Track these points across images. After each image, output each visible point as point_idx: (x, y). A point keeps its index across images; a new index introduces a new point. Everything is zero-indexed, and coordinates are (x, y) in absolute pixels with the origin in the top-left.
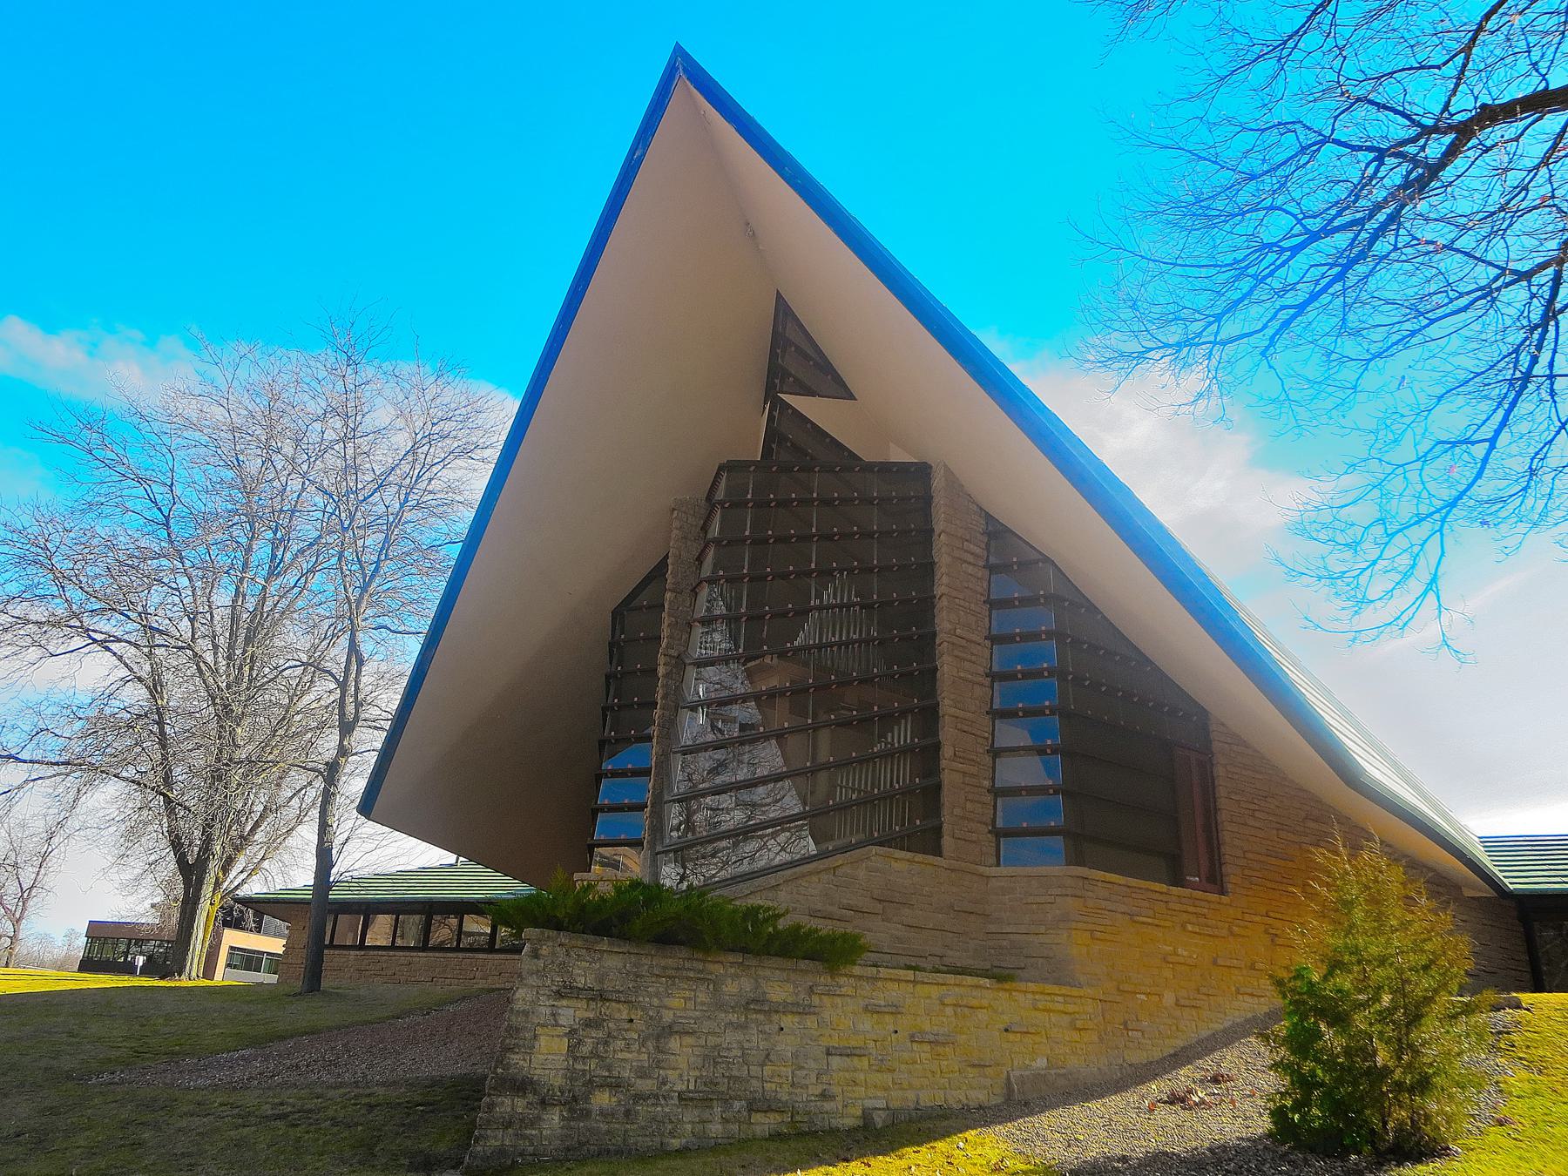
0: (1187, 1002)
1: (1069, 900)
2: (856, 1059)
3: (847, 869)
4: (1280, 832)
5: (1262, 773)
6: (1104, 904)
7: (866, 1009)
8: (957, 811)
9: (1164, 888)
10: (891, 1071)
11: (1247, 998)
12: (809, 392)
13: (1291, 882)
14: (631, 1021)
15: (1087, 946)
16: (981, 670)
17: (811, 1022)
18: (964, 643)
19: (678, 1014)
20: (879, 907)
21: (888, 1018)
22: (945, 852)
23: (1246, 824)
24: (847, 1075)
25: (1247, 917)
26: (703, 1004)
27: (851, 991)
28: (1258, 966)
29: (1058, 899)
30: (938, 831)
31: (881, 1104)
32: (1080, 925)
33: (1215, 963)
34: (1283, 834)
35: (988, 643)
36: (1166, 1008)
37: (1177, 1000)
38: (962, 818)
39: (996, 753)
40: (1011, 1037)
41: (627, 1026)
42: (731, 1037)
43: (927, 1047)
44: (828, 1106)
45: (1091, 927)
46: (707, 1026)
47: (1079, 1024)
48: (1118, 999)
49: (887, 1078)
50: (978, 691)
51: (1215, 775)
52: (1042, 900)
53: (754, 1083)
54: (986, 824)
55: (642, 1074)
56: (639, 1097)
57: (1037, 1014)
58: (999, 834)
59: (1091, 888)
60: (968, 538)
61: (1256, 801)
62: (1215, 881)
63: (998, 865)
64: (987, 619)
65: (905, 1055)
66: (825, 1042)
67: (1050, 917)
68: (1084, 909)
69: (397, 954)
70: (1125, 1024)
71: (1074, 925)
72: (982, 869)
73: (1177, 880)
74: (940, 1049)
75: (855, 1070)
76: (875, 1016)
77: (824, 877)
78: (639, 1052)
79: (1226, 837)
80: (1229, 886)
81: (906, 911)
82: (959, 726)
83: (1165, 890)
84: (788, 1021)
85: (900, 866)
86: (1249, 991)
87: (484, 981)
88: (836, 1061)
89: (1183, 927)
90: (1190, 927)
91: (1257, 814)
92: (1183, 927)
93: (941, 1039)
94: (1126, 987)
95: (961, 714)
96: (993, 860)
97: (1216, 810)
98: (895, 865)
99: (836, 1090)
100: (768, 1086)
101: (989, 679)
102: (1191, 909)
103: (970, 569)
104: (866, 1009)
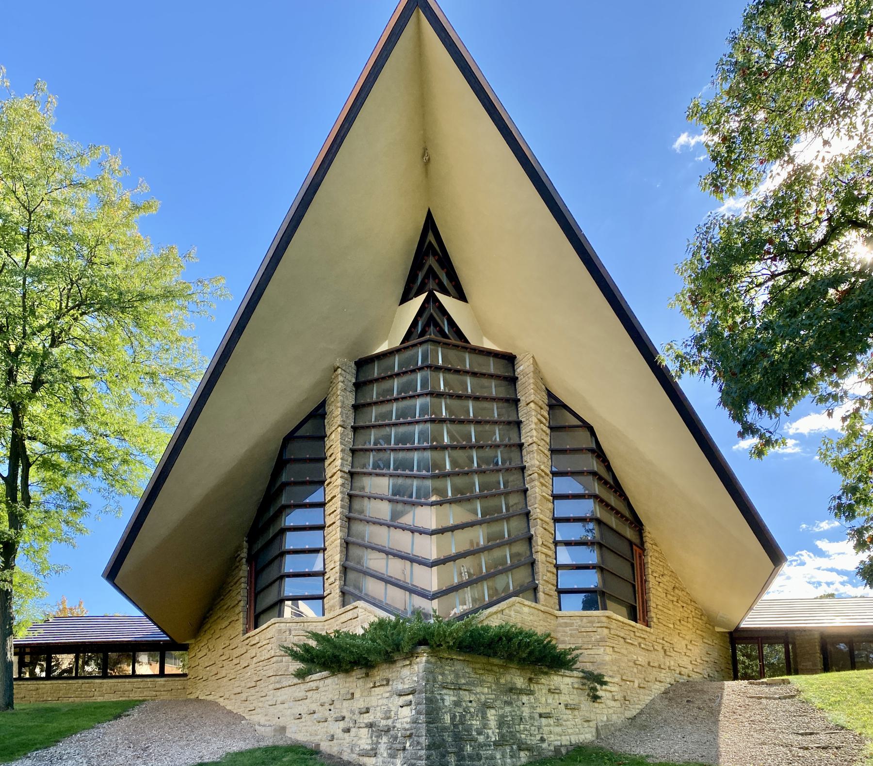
1: (604, 629)
8: (545, 578)
10: (561, 725)
14: (471, 702)
21: (556, 696)
26: (495, 690)
29: (599, 630)
30: (535, 589)
31: (559, 743)
33: (649, 663)
41: (470, 704)
42: (508, 709)
44: (545, 745)
45: (613, 645)
46: (498, 703)
52: (590, 629)
56: (481, 746)
58: (560, 592)
63: (560, 610)
66: (540, 710)
67: (593, 639)
70: (625, 697)
73: (633, 617)
75: (549, 725)
77: (499, 615)
80: (652, 623)
82: (544, 526)
84: (525, 699)
88: (543, 720)
92: (640, 644)
93: (576, 707)
94: (624, 678)
96: (558, 607)
97: (646, 581)
100: (523, 736)
104: (549, 690)
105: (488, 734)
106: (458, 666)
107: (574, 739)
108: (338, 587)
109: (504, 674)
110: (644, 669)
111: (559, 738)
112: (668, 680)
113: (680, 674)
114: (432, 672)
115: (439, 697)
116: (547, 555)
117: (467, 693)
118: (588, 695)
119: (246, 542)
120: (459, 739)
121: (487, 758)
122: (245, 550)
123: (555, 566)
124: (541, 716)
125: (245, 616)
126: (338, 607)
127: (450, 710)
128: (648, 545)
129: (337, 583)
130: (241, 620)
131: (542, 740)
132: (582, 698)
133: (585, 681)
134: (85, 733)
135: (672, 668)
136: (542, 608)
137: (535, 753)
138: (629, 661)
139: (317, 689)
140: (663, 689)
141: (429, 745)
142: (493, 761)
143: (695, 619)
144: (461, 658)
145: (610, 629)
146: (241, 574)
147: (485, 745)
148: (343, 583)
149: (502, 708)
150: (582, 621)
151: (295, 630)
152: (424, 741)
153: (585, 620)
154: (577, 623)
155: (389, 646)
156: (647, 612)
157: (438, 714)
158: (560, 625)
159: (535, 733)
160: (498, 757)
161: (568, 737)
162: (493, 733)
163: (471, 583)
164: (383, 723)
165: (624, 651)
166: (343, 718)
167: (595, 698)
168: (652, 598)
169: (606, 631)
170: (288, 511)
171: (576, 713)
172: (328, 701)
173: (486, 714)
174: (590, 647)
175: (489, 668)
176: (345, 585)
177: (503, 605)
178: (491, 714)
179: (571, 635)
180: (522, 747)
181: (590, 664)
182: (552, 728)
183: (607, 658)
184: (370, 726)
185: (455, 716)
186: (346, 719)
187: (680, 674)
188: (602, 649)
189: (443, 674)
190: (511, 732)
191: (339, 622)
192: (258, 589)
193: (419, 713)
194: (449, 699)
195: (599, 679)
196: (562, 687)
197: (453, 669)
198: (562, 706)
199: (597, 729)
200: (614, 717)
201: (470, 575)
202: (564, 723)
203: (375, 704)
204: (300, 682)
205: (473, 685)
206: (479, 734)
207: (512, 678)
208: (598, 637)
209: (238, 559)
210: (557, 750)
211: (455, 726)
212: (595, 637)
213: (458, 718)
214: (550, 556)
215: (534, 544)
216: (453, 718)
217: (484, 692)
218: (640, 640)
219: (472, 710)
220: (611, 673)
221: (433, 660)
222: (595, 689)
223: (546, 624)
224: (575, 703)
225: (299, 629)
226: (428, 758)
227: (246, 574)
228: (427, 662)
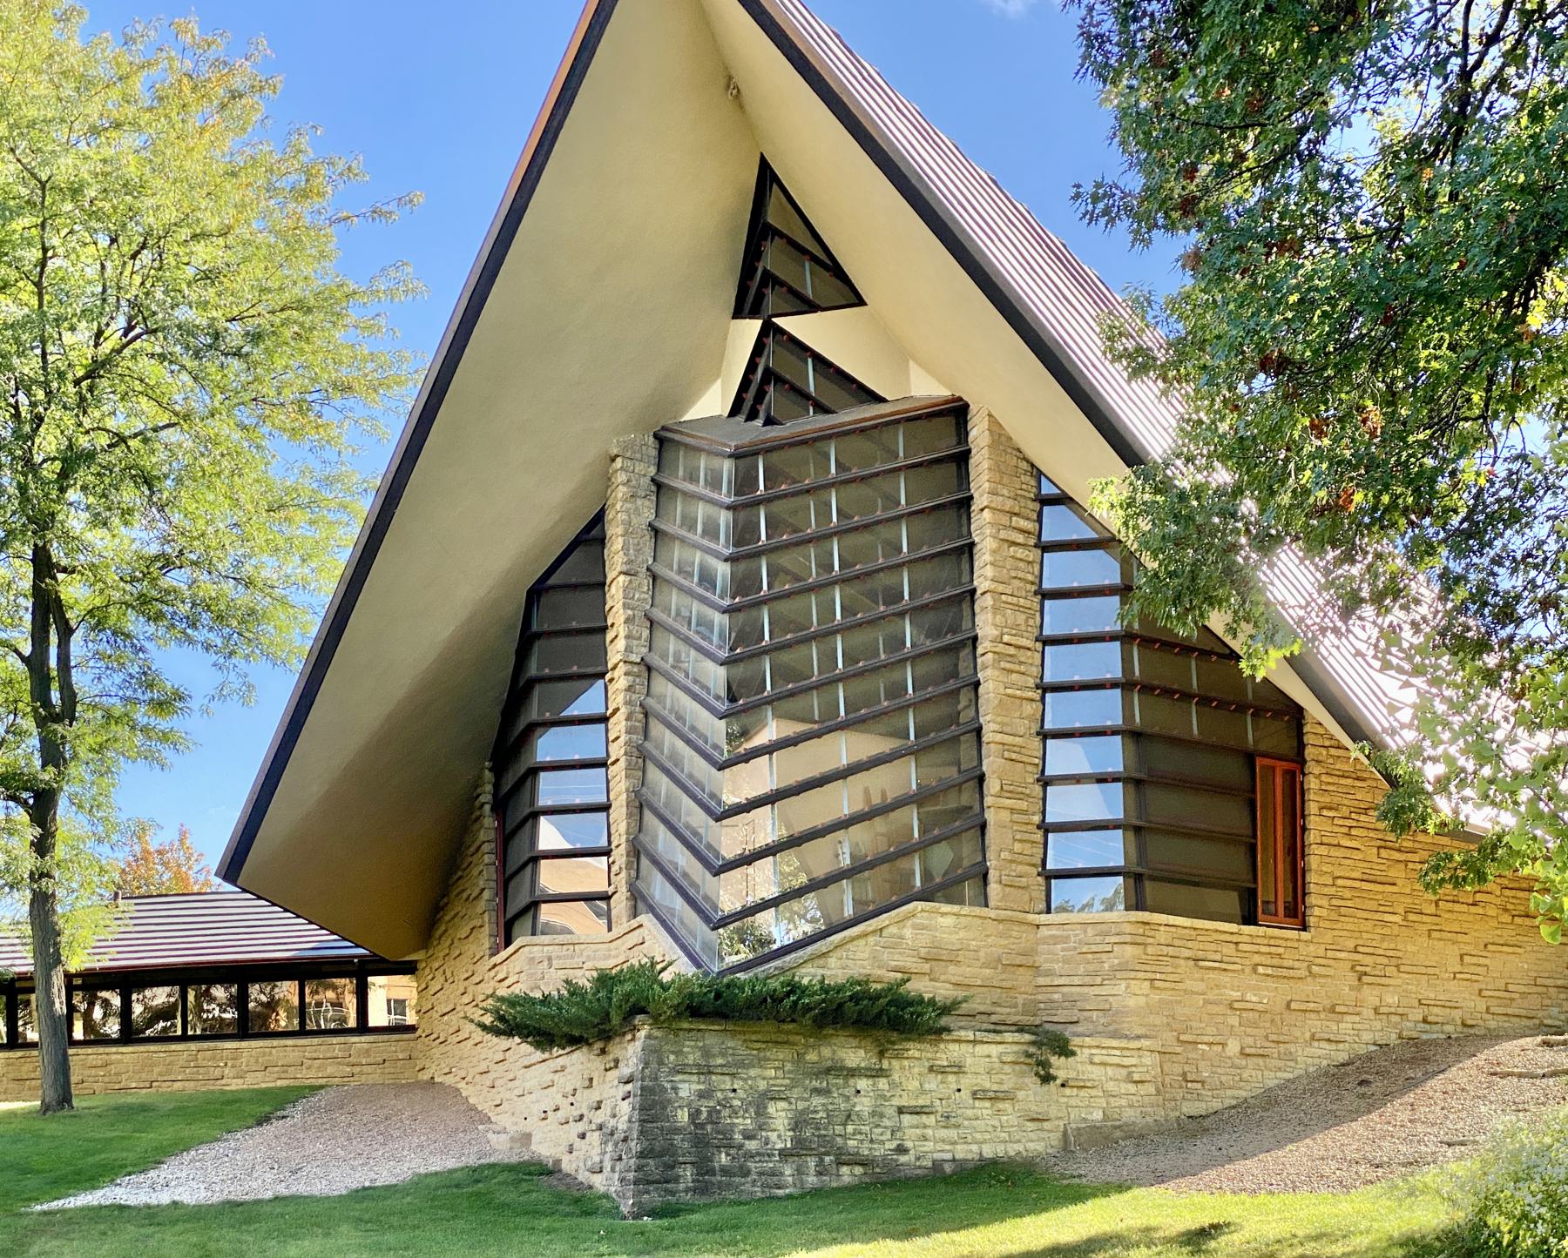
0: (1253, 1051)
1: (1129, 948)
2: (924, 1117)
3: (893, 930)
4: (1382, 850)
5: (1364, 780)
6: (1166, 950)
7: (931, 1069)
9: (1233, 927)
10: (957, 1126)
11: (1324, 1045)
12: (810, 307)
13: (1387, 909)
14: (734, 1091)
15: (1147, 996)
16: (1031, 682)
17: (882, 1083)
18: (1012, 651)
19: (771, 1082)
20: (926, 967)
21: (951, 1078)
22: (992, 903)
23: (1339, 845)
24: (918, 1131)
25: (1330, 954)
26: (790, 1072)
27: (917, 1054)
28: (1338, 1009)
31: (948, 1156)
32: (1140, 975)
33: (1288, 1006)
34: (1384, 853)
35: (1039, 646)
36: (1230, 1058)
37: (1242, 1048)
38: (1012, 861)
39: (1045, 782)
40: (1067, 1091)
41: (732, 1095)
42: (817, 1101)
43: (987, 1104)
44: (903, 1159)
45: (1150, 975)
46: (796, 1093)
47: (1136, 1077)
48: (1179, 1050)
49: (952, 1134)
51: (1306, 787)
53: (838, 1139)
54: (1034, 865)
55: (749, 1136)
56: (750, 1155)
57: (1090, 1067)
58: (1050, 876)
59: (1152, 933)
60: (1017, 510)
61: (1353, 816)
62: (1296, 914)
63: (1048, 911)
64: (1038, 614)
65: (970, 1113)
66: (896, 1102)
68: (1144, 957)
69: (80, 1051)
70: (1184, 1074)
71: (1133, 974)
72: (1031, 917)
74: (1001, 1105)
75: (925, 1127)
76: (939, 1077)
77: (871, 939)
78: (744, 1118)
79: (1313, 862)
81: (952, 968)
82: (1006, 754)
83: (1235, 930)
84: (862, 1084)
86: (1327, 1036)
87: (240, 1081)
88: (906, 1119)
89: (1255, 970)
90: (1261, 970)
91: (1354, 832)
92: (1255, 970)
95: (1009, 739)
96: (1043, 906)
97: (1304, 829)
98: (940, 919)
99: (909, 1144)
101: (1040, 691)
102: (1264, 949)
103: (1021, 553)
104: (931, 1069)
105: (767, 1138)
106: (711, 1040)
107: (988, 1152)
108: (624, 881)
109: (813, 1047)
110: (1268, 1015)
111: (948, 1147)
112: (1367, 1037)
113: (1425, 1021)
114: (656, 1051)
115: (668, 1086)
116: (1012, 810)
117: (727, 1078)
118: (1037, 1074)
119: (490, 770)
120: (701, 1143)
121: (761, 1174)
122: (489, 788)
123: (1039, 827)
125: (494, 919)
126: (624, 919)
127: (689, 1105)
128: (1309, 752)
129: (623, 874)
130: (486, 930)
131: (901, 1150)
132: (1027, 1080)
133: (1032, 1050)
134: (203, 1149)
135: (1382, 1010)
136: (992, 914)
137: (878, 1170)
138: (1207, 1002)
139: (563, 1069)
140: (1343, 1057)
141: (641, 1152)
142: (775, 1178)
143: (1507, 892)
144: (717, 1027)
145: (1145, 945)
146: (482, 836)
147: (758, 1154)
148: (633, 873)
149: (806, 1100)
150: (1085, 932)
151: (559, 957)
152: (635, 1146)
153: (1090, 931)
154: (1076, 935)
155: (595, 1016)
156: (1304, 894)
157: (664, 1108)
158: (1045, 941)
159: (883, 1138)
160: (787, 1173)
161: (975, 1148)
162: (779, 1136)
163: (814, 886)
164: (612, 1122)
165: (1200, 987)
166: (581, 1117)
167: (1047, 1079)
168: (1314, 866)
170: (539, 730)
171: (1006, 1105)
172: (569, 1089)
173: (766, 1108)
174: (1099, 980)
175: (784, 1038)
176: (637, 877)
177: (884, 919)
178: (779, 1114)
179: (1066, 961)
181: (1100, 1013)
182: (930, 1132)
183: (1132, 1002)
184: (600, 1127)
185: (698, 1112)
186: (585, 1119)
187: (1425, 1021)
188: (1123, 984)
189: (678, 1053)
190: (818, 1136)
191: (624, 948)
192: (509, 872)
193: (633, 1108)
194: (688, 1088)
195: (1064, 1050)
196: (969, 1061)
197: (701, 1044)
198: (966, 1094)
199: (1065, 1134)
200: (1130, 1115)
201: (852, 857)
202: (966, 1123)
203: (606, 1096)
204: (547, 1055)
205: (742, 1065)
206: (749, 1136)
207: (834, 1052)
208: (1116, 961)
209: (477, 804)
210: (937, 1165)
211: (702, 1126)
213: (704, 1115)
214: (1024, 812)
215: (985, 792)
217: (765, 1076)
218: (1257, 959)
219: (737, 1103)
220: (1140, 1031)
221: (657, 1033)
222: (1045, 1064)
223: (1003, 942)
224: (1005, 1087)
225: (565, 957)
226: (639, 1169)
227: (492, 835)
228: (648, 1037)
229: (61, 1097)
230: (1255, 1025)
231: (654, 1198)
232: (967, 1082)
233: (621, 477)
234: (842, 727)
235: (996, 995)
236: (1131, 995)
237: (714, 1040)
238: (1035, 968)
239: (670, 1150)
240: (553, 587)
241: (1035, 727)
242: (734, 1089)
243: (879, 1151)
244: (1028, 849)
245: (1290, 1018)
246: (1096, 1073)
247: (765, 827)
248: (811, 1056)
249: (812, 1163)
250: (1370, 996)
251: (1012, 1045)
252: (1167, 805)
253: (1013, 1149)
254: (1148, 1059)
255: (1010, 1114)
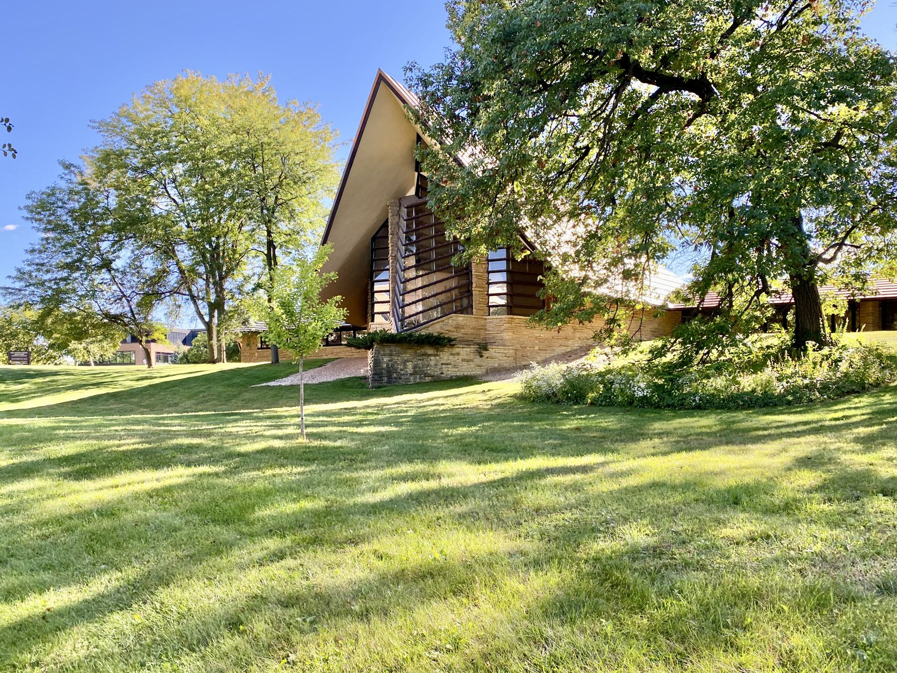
17: (438, 358)
42: (420, 362)
49: (456, 370)
50: (484, 266)
56: (402, 375)
84: (432, 358)
85: (461, 318)
88: (443, 366)
106: (393, 348)
107: (465, 374)
112: (576, 345)
124: (442, 364)
131: (442, 373)
167: (481, 356)
169: (507, 325)
178: (410, 365)
180: (427, 375)
183: (507, 337)
195: (486, 350)
198: (460, 360)
212: (503, 328)
216: (388, 365)
217: (407, 356)
222: (480, 353)
229: (276, 361)
230: (543, 342)
231: (376, 384)
232: (460, 357)
233: (390, 211)
234: (434, 272)
235: (473, 336)
236: (507, 336)
237: (394, 348)
238: (486, 330)
239: (381, 373)
240: (380, 237)
241: (486, 270)
242: (398, 359)
243: (436, 374)
244: (484, 300)
245: (553, 340)
246: (497, 355)
247: (420, 294)
248: (419, 351)
249: (418, 376)
250: (578, 335)
251: (473, 348)
252: (519, 289)
253: (472, 373)
254: (511, 351)
255: (472, 365)
